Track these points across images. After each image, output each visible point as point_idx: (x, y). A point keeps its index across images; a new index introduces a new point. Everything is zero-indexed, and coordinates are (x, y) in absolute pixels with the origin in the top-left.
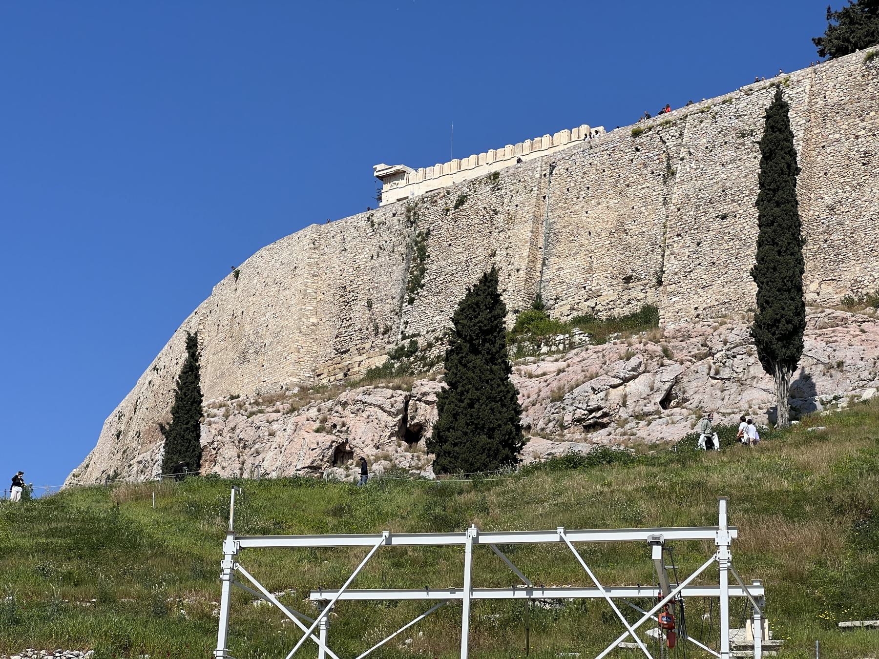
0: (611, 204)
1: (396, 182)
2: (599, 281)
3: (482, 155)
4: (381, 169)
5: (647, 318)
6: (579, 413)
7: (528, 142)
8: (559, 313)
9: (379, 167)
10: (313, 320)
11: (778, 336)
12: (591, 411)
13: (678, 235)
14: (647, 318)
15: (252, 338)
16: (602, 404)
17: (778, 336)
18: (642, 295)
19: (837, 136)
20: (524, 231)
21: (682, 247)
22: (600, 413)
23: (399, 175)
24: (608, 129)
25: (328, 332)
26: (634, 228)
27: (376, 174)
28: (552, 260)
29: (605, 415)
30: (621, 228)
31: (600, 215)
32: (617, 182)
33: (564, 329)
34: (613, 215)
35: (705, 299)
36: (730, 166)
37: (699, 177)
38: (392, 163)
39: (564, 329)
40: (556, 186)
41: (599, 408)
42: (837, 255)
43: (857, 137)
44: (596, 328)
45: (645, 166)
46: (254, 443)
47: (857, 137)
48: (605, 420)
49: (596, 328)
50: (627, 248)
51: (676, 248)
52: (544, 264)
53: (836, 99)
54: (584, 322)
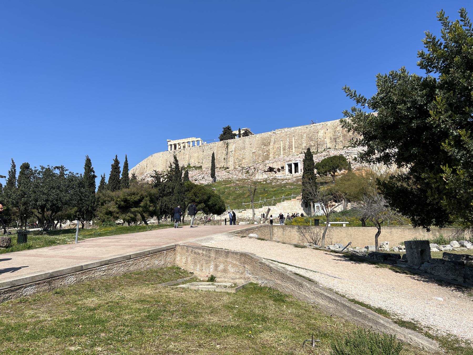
2: (196, 162)
4: (168, 140)
5: (201, 167)
8: (192, 165)
11: (213, 175)
14: (201, 167)
17: (213, 175)
20: (187, 156)
21: (205, 160)
25: (164, 164)
31: (196, 155)
33: (192, 167)
35: (207, 166)
39: (192, 167)
40: (191, 151)
44: (196, 168)
49: (196, 168)
54: (194, 167)
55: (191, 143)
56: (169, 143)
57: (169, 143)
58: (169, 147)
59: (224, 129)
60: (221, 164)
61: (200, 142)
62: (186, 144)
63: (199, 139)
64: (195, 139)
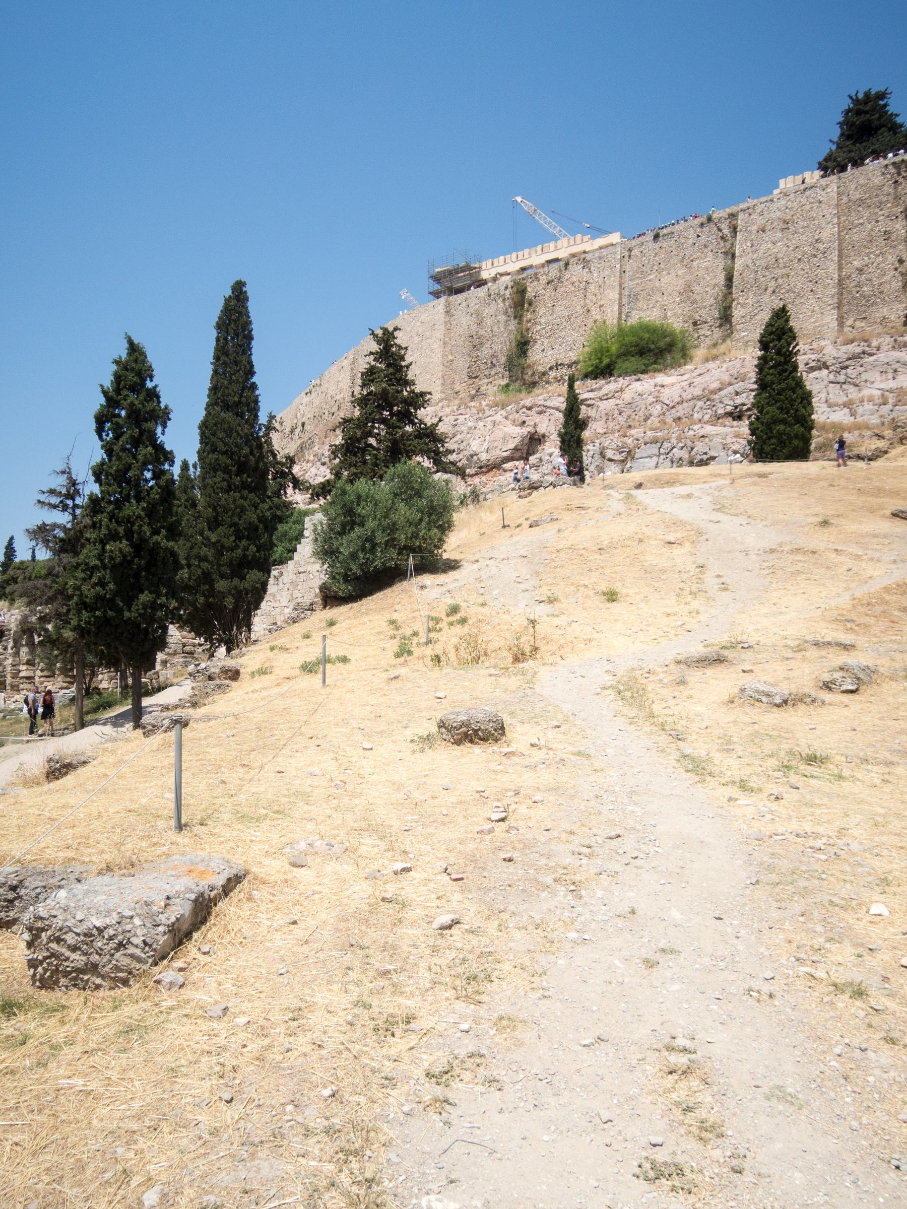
0: (680, 273)
3: (508, 257)
6: (729, 409)
7: (539, 248)
10: (450, 357)
13: (743, 291)
18: (709, 333)
19: (861, 221)
24: (593, 238)
26: (697, 289)
28: (634, 312)
30: (688, 289)
32: (683, 258)
34: (681, 281)
42: (868, 301)
43: (878, 221)
45: (705, 246)
46: (454, 436)
47: (878, 221)
50: (694, 302)
51: (741, 300)
52: (627, 316)
53: (858, 196)
59: (856, 101)
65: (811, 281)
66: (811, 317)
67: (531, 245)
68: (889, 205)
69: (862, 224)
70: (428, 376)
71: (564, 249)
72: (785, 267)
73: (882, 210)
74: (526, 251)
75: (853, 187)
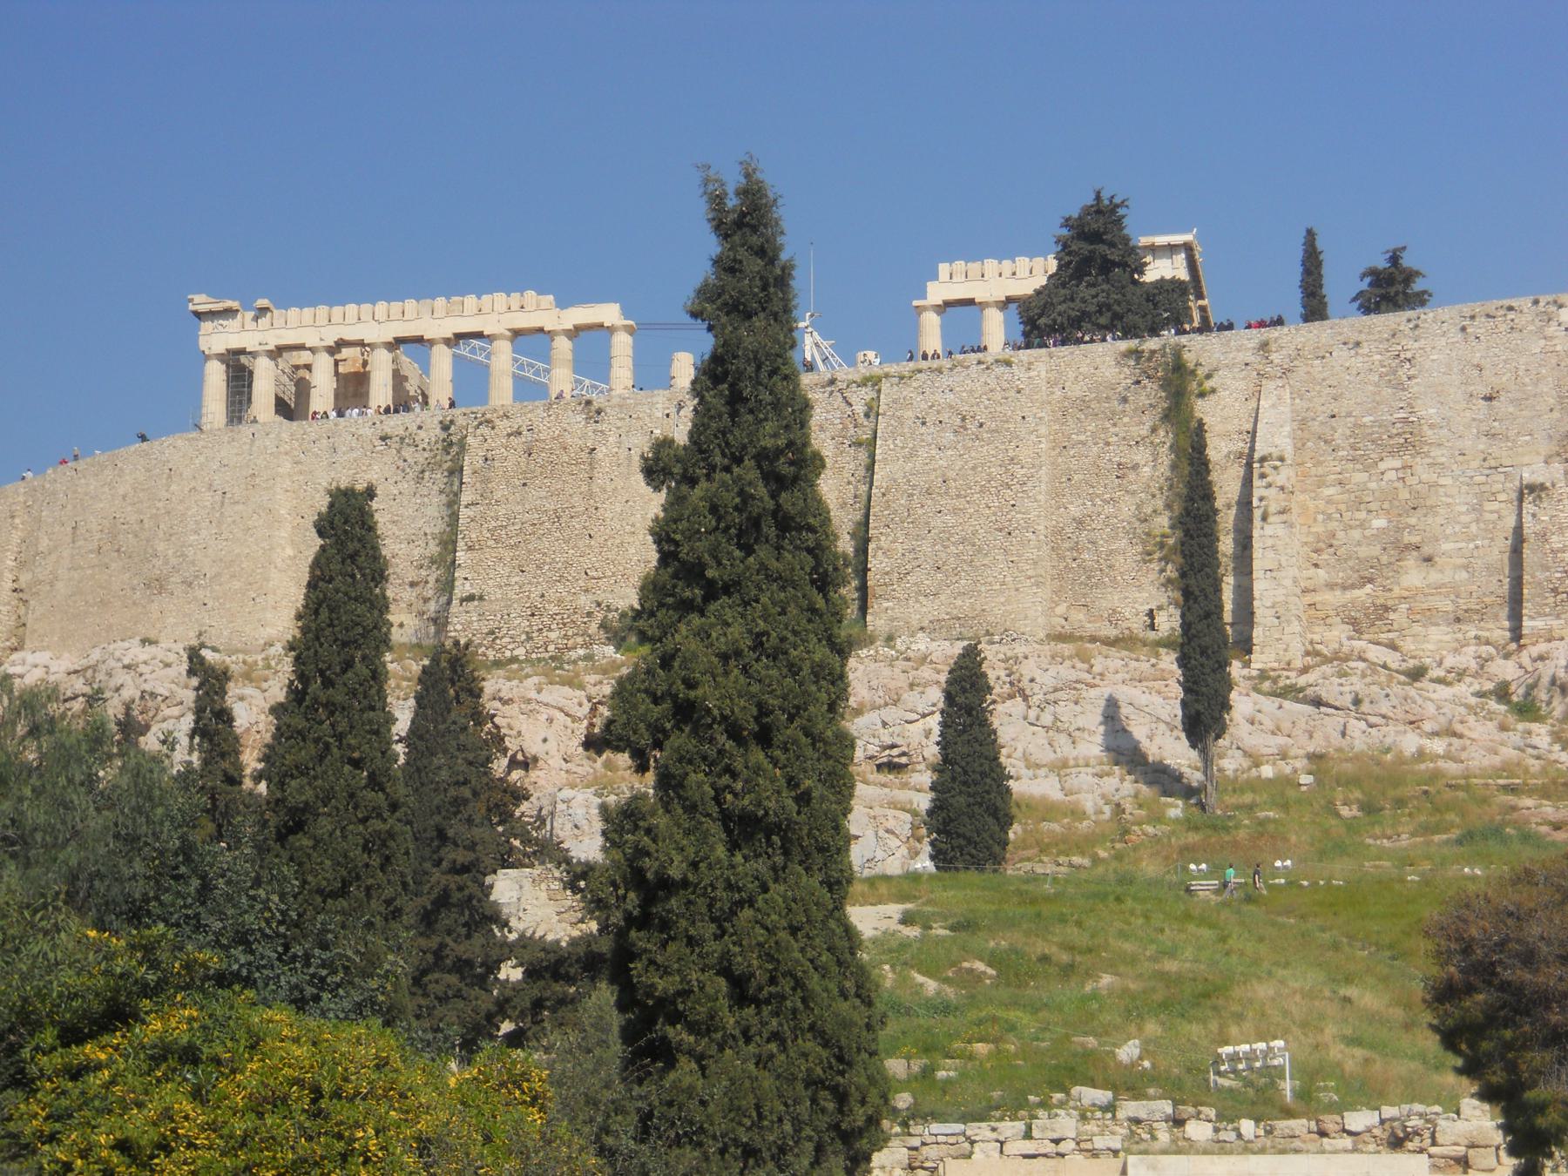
1: (224, 323)
3: (366, 307)
4: (201, 302)
7: (440, 302)
9: (198, 298)
12: (884, 748)
15: (173, 561)
16: (899, 741)
19: (1082, 438)
22: (895, 752)
23: (229, 313)
24: (562, 304)
27: (191, 307)
29: (904, 754)
36: (950, 452)
37: (907, 458)
38: (218, 295)
41: (893, 746)
42: (1089, 578)
43: (1108, 444)
47: (1108, 444)
48: (904, 760)
51: (884, 541)
53: (1078, 394)
55: (442, 360)
56: (217, 338)
57: (217, 338)
58: (216, 375)
60: (1110, 599)
61: (622, 344)
62: (502, 358)
63: (609, 313)
64: (539, 311)
65: (1000, 530)
66: (1002, 592)
67: (423, 292)
68: (1126, 420)
69: (1083, 443)
70: (237, 585)
71: (495, 316)
72: (958, 496)
73: (1115, 425)
74: (410, 304)
75: (1071, 375)
